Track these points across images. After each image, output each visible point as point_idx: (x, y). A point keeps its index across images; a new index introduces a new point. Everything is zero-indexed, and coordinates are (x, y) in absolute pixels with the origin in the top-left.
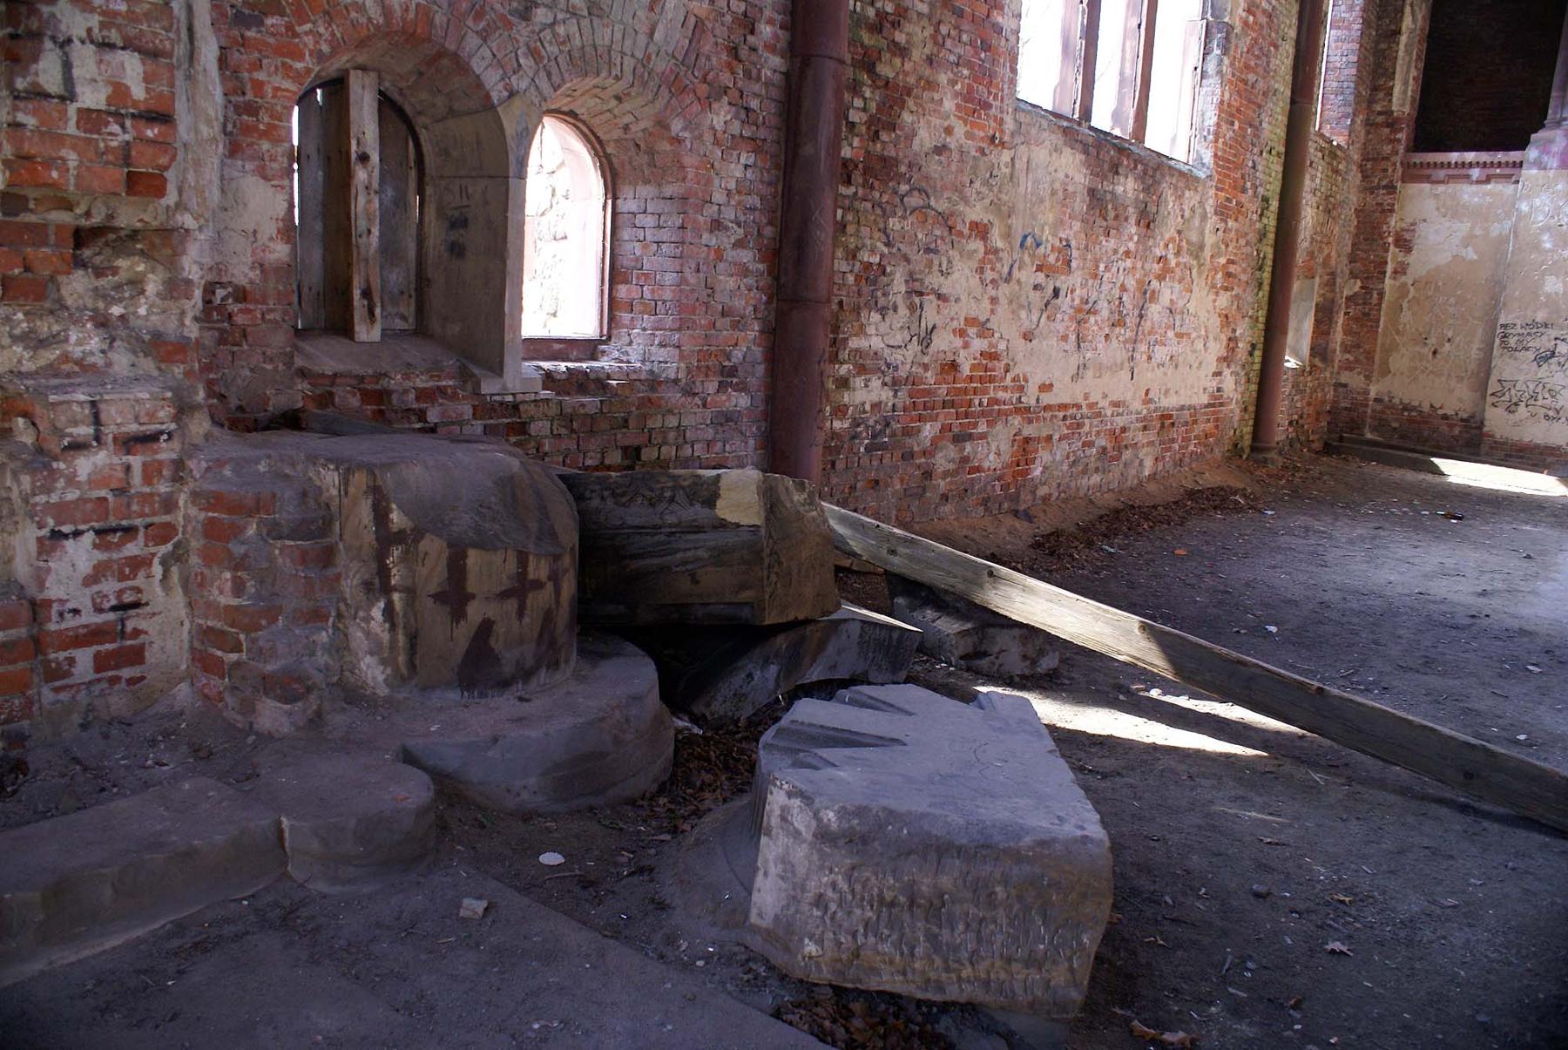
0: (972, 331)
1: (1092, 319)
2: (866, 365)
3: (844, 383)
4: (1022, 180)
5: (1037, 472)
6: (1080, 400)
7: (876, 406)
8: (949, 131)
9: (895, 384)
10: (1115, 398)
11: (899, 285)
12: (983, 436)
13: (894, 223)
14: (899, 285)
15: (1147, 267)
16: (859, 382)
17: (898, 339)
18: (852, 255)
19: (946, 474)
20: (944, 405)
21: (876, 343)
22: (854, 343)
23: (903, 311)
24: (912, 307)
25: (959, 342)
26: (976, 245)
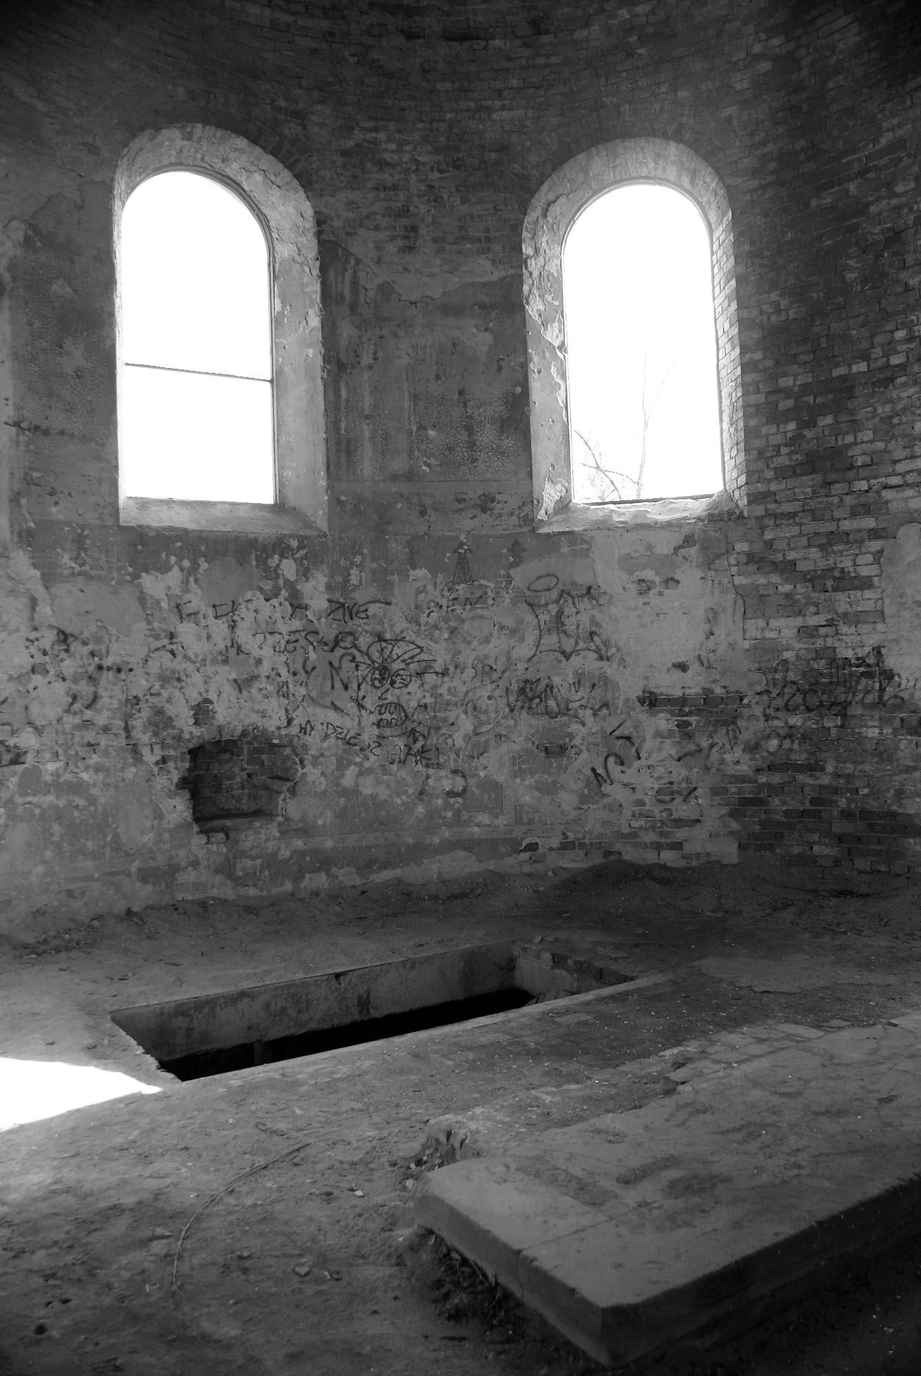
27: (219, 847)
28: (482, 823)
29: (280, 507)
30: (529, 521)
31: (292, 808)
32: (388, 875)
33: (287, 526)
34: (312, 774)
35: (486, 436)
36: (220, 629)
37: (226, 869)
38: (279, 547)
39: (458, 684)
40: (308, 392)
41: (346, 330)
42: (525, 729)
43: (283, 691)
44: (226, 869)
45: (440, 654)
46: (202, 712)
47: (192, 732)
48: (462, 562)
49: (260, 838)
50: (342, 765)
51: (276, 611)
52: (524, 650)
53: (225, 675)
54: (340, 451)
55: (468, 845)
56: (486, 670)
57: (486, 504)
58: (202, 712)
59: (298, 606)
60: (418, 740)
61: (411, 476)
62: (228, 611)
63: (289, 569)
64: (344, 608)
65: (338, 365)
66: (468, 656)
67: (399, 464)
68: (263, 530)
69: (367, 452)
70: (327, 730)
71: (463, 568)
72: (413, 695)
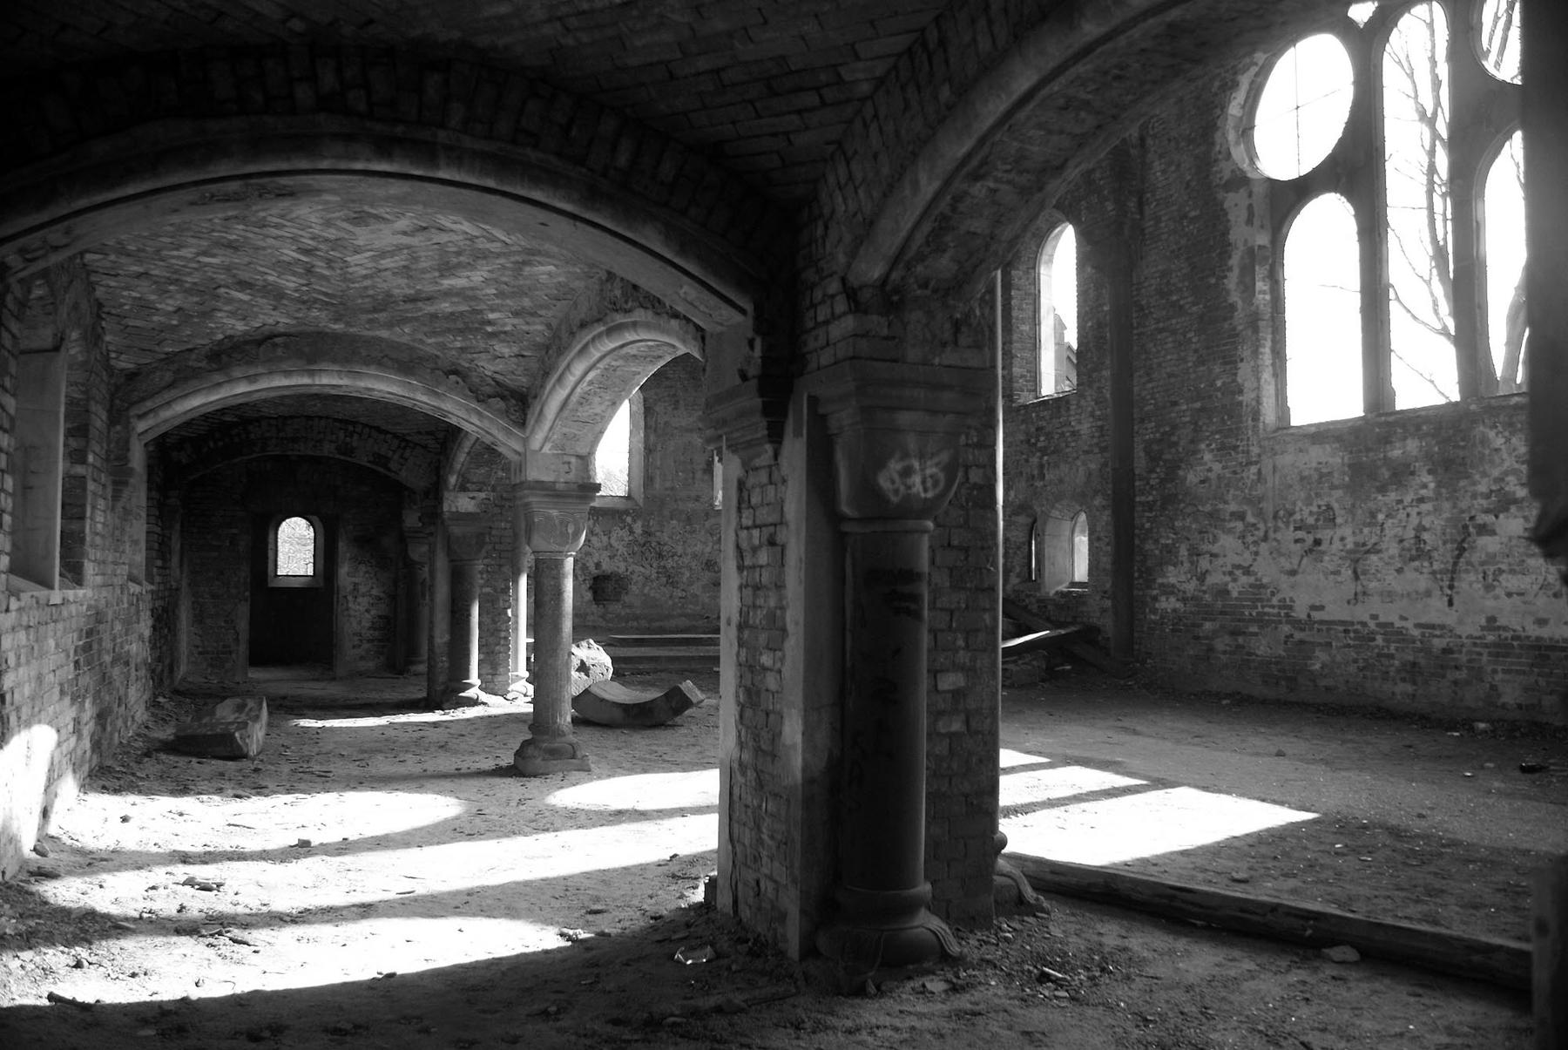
0: (1238, 572)
1: (1374, 558)
2: (1169, 590)
3: (1155, 599)
4: (1270, 479)
5: (1317, 666)
6: (1366, 618)
7: (1174, 610)
8: (1210, 470)
9: (1184, 600)
10: (1423, 621)
11: (1183, 552)
12: (1256, 634)
13: (1178, 524)
14: (1183, 552)
15: (1463, 505)
16: (1163, 598)
17: (1183, 578)
18: (1156, 541)
19: (1225, 652)
20: (1222, 613)
21: (1172, 580)
22: (1160, 581)
23: (1187, 565)
24: (1192, 563)
25: (1228, 578)
26: (1239, 525)
27: (601, 610)
28: (690, 609)
29: (629, 497)
30: (712, 505)
31: (626, 598)
32: (658, 624)
33: (630, 505)
34: (634, 588)
35: (699, 475)
36: (605, 539)
37: (603, 617)
38: (626, 512)
39: (686, 560)
40: (639, 458)
41: (652, 438)
42: (708, 575)
43: (625, 560)
44: (603, 617)
45: (680, 550)
46: (598, 565)
47: (595, 572)
48: (689, 519)
49: (615, 608)
50: (644, 585)
51: (624, 533)
52: (708, 549)
53: (606, 554)
54: (648, 480)
55: (686, 616)
56: (695, 556)
57: (697, 499)
58: (598, 565)
59: (631, 532)
60: (671, 579)
61: (672, 489)
62: (608, 533)
63: (629, 519)
64: (647, 533)
65: (649, 450)
66: (689, 551)
67: (668, 484)
68: (621, 506)
69: (658, 480)
70: (639, 572)
71: (689, 520)
72: (670, 563)
